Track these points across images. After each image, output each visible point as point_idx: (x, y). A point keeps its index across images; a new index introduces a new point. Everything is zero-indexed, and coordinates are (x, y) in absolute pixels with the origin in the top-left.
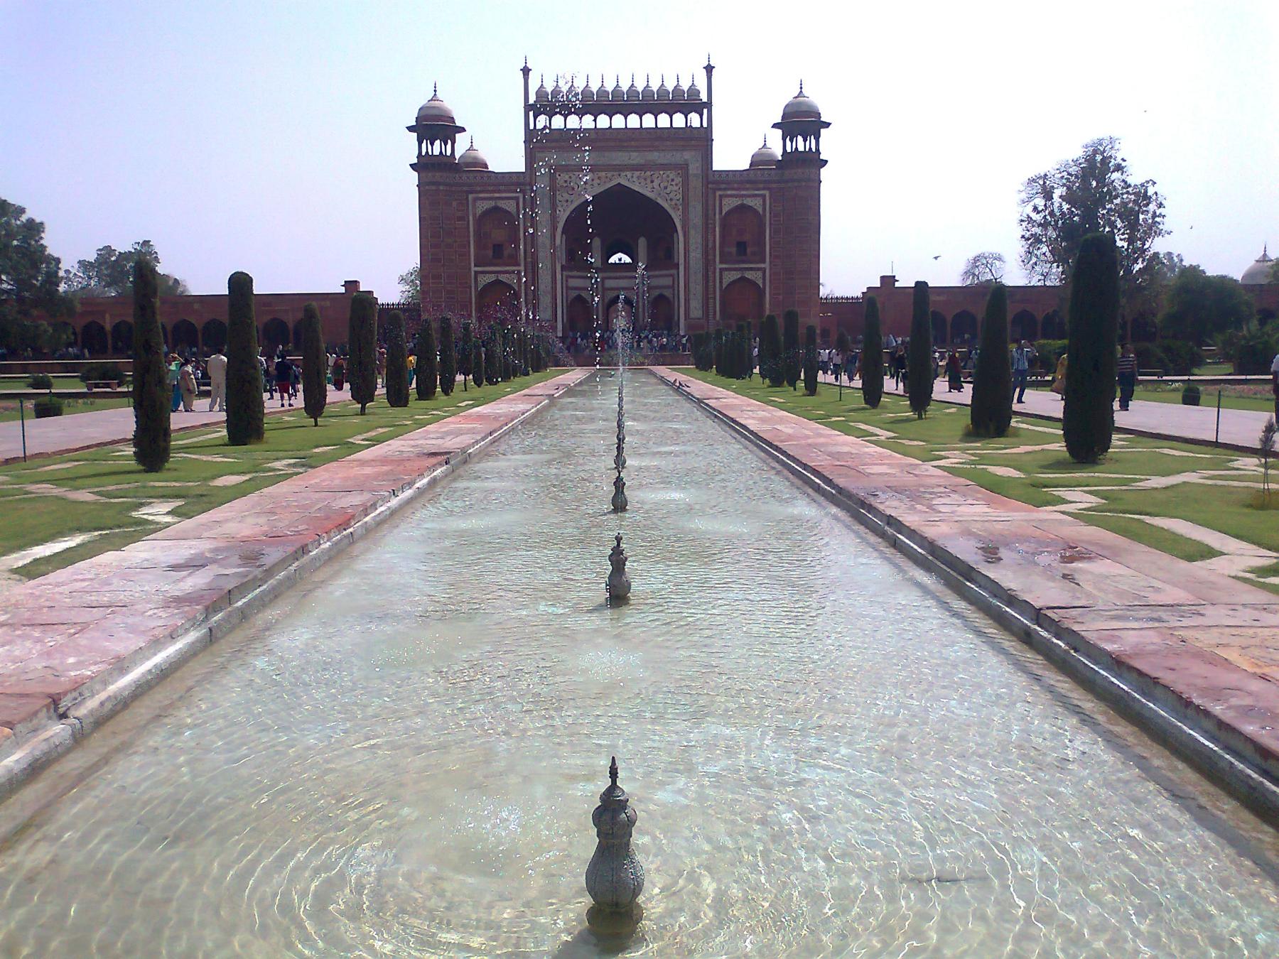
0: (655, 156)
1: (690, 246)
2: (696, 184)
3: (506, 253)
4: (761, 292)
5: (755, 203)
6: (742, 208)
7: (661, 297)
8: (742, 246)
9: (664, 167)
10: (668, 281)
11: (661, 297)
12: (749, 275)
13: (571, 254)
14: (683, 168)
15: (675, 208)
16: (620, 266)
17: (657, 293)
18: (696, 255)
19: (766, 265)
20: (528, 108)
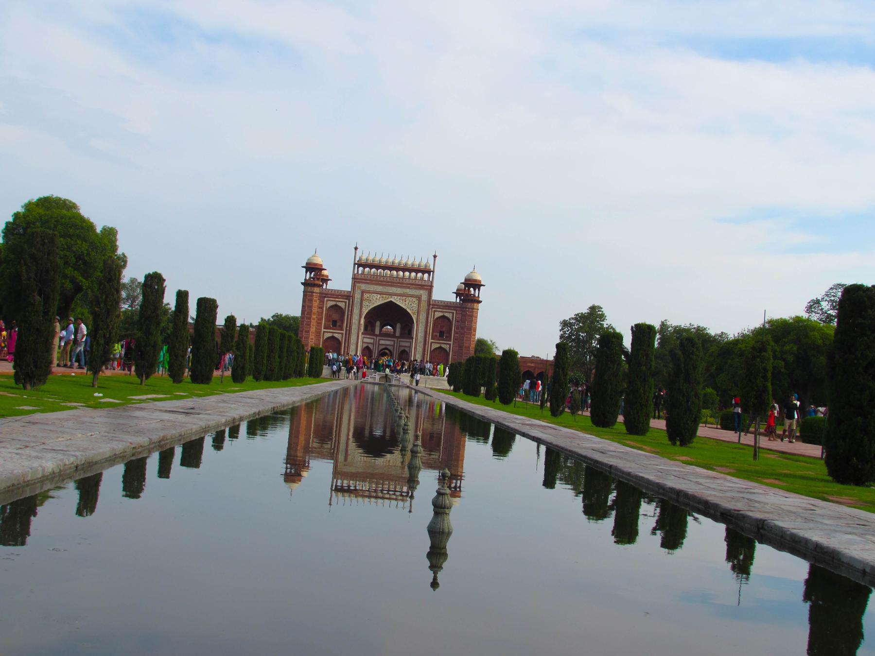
0: (408, 291)
1: (419, 331)
2: (424, 305)
3: (338, 324)
4: (448, 354)
5: (449, 315)
6: (443, 317)
7: (404, 351)
8: (442, 334)
9: (412, 296)
10: (407, 344)
11: (404, 351)
12: (443, 346)
13: (366, 328)
14: (419, 298)
15: (414, 314)
16: (387, 335)
17: (402, 349)
18: (421, 335)
19: (451, 343)
20: (355, 264)
